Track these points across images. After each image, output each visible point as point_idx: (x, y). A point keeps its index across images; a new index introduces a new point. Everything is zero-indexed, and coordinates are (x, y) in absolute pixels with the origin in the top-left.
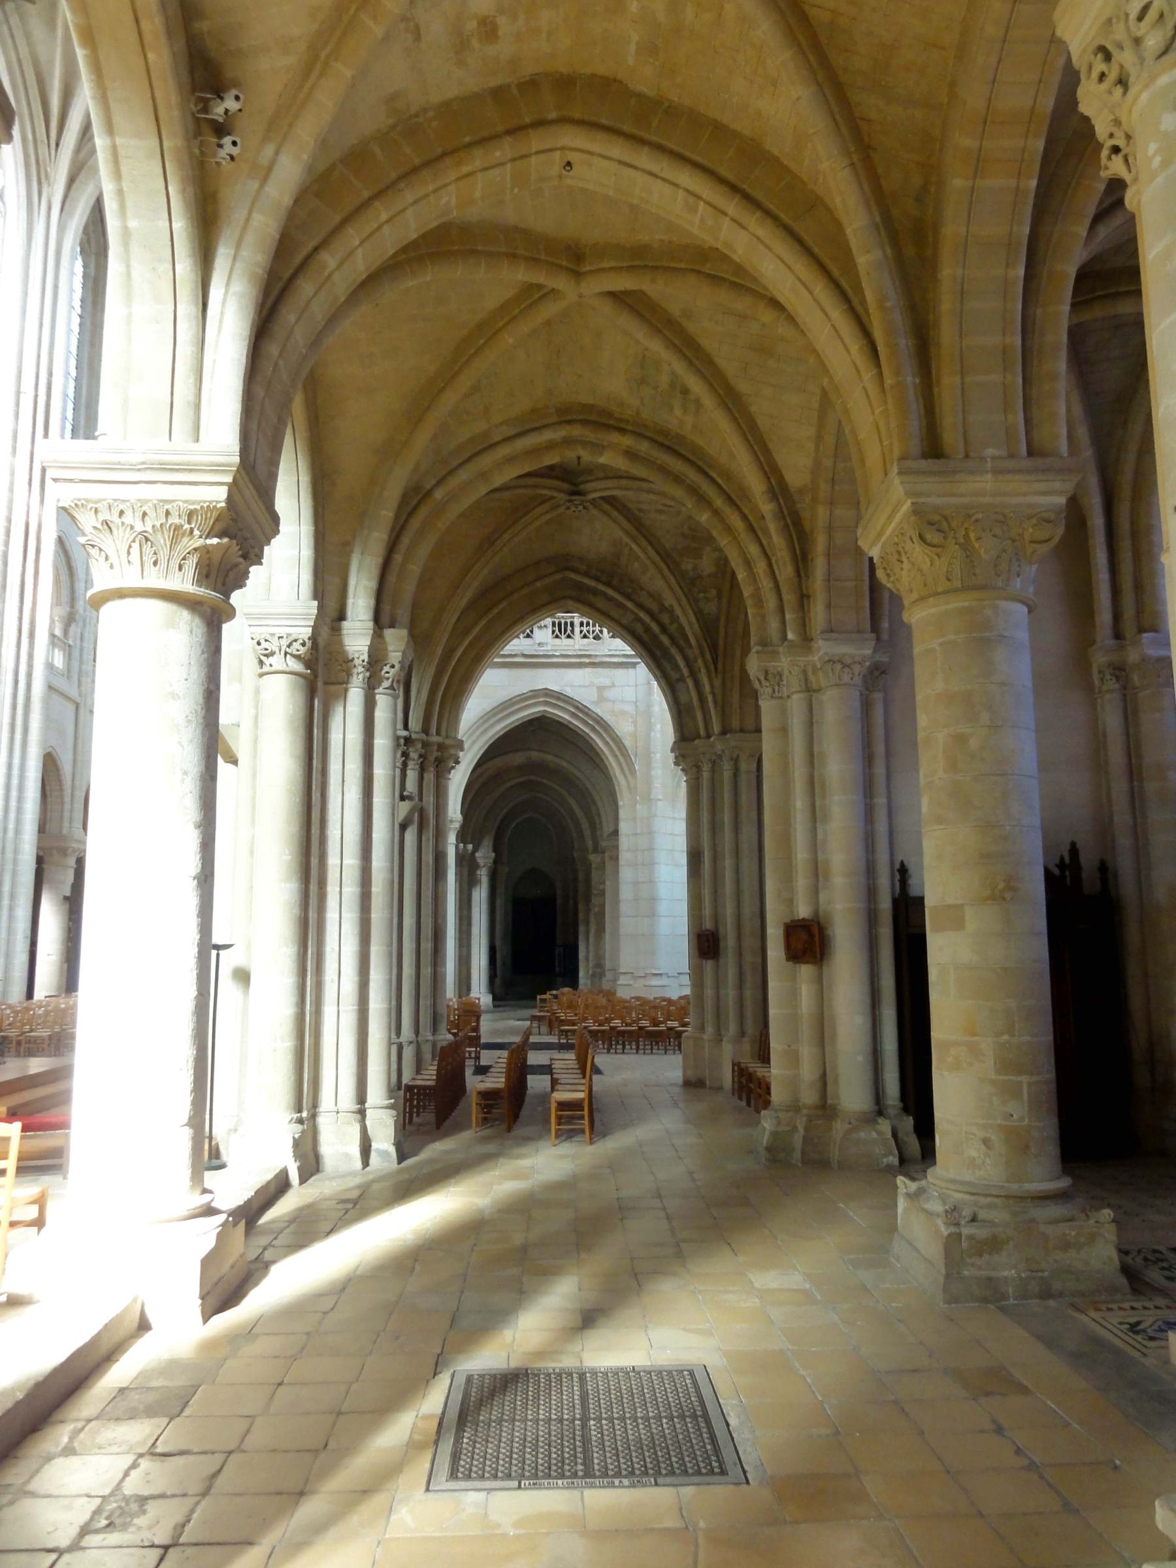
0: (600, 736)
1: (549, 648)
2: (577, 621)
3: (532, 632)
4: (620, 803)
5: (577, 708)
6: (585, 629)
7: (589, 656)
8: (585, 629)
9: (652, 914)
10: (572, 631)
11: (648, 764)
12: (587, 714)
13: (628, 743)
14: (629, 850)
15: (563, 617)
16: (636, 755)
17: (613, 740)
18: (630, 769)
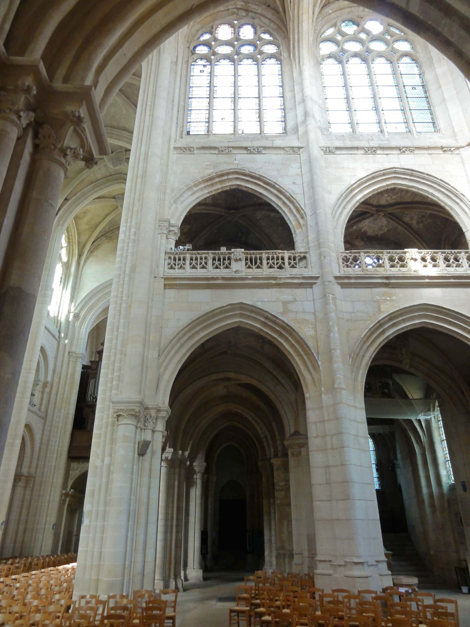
0: (286, 339)
1: (243, 274)
2: (264, 256)
3: (230, 264)
4: (307, 395)
5: (267, 318)
6: (271, 262)
7: (275, 278)
8: (271, 262)
9: (347, 498)
10: (261, 263)
11: (330, 360)
12: (275, 323)
13: (311, 344)
14: (317, 437)
15: (253, 254)
16: (318, 354)
17: (298, 342)
18: (313, 366)
